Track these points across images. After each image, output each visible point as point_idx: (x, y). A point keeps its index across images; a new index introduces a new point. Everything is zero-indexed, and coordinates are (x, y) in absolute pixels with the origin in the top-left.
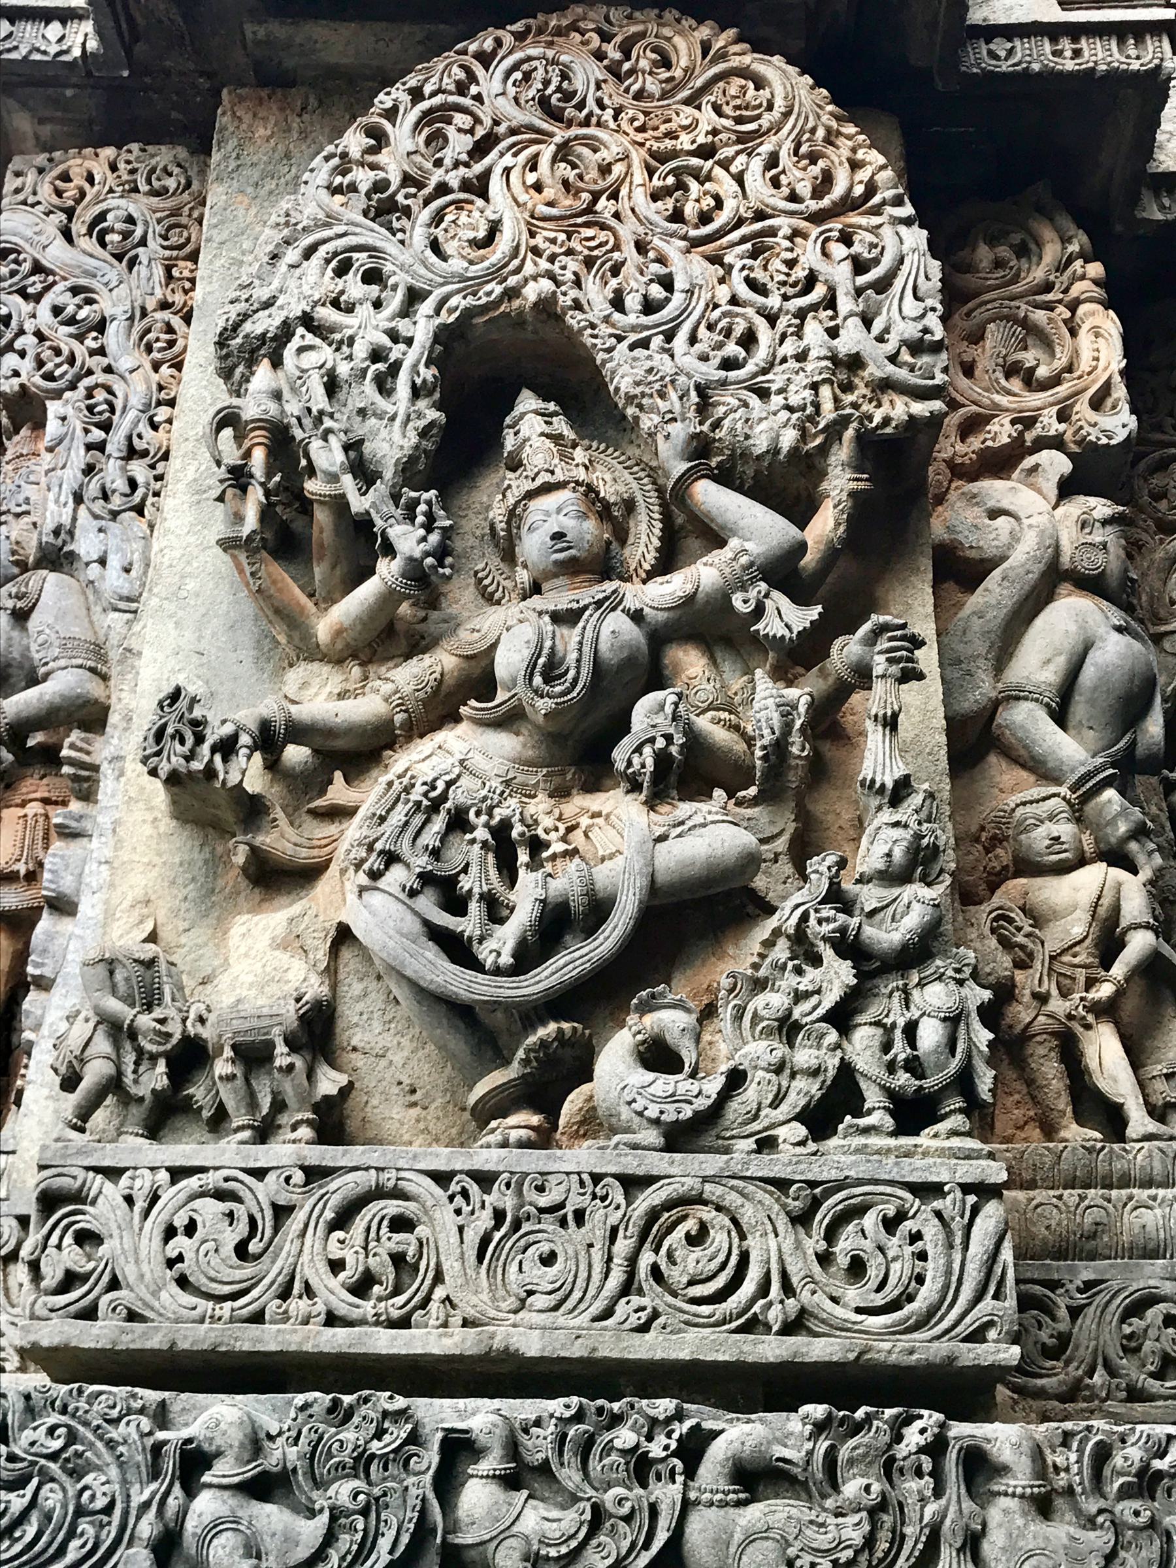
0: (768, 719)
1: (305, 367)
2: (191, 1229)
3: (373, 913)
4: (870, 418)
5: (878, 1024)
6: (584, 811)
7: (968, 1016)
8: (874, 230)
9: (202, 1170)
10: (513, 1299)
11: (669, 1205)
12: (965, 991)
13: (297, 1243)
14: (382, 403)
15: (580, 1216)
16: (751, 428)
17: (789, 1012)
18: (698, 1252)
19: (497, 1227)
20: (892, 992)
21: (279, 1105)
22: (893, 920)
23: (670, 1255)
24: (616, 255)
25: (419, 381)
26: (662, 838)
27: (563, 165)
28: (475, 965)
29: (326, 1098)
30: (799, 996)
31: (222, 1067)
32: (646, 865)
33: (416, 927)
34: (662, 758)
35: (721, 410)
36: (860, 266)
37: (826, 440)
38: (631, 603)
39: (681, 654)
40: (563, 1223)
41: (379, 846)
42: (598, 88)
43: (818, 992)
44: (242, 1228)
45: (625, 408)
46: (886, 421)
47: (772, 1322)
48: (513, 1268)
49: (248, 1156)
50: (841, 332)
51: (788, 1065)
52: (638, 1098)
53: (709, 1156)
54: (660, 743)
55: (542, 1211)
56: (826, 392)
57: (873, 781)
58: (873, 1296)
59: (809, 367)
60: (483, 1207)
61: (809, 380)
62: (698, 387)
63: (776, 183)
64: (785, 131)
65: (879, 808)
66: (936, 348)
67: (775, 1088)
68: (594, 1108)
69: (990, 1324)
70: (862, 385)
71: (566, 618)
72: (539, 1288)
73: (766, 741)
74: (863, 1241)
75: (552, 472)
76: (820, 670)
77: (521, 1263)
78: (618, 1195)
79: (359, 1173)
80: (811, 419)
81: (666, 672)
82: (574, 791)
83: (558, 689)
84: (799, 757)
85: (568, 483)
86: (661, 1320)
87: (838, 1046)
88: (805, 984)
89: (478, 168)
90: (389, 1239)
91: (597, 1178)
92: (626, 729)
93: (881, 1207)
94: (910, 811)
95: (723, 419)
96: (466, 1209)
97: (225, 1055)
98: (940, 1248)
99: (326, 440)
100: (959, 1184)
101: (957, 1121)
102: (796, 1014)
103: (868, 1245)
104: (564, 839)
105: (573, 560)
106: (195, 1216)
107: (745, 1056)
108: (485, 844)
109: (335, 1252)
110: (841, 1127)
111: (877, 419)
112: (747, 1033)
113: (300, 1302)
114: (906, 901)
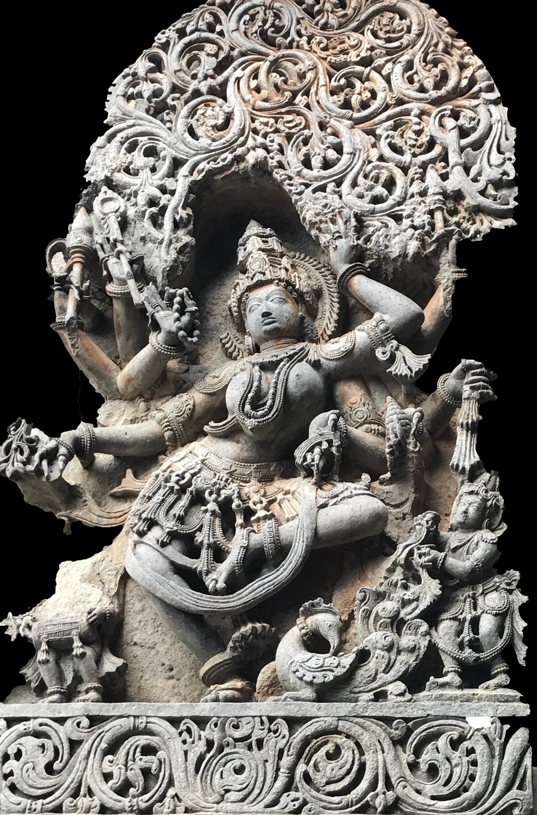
0: (393, 429)
1: (106, 211)
2: (18, 755)
3: (139, 558)
4: (467, 232)
5: (455, 619)
6: (280, 490)
7: (513, 612)
8: (474, 108)
9: (27, 719)
10: (216, 795)
11: (316, 735)
12: (511, 597)
13: (83, 763)
14: (154, 232)
15: (260, 743)
16: (389, 241)
17: (398, 613)
18: (333, 764)
19: (208, 750)
20: (465, 599)
21: (78, 679)
22: (467, 554)
23: (316, 766)
24: (306, 132)
25: (178, 218)
26: (324, 506)
27: (274, 74)
28: (203, 589)
29: (109, 674)
30: (405, 603)
31: (41, 656)
32: (312, 523)
33: (166, 565)
34: (326, 454)
35: (371, 229)
36: (463, 133)
37: (437, 247)
38: (312, 357)
39: (346, 388)
40: (250, 748)
41: (144, 516)
42: (298, 22)
43: (417, 599)
44: (50, 754)
45: (310, 231)
46: (478, 232)
47: (377, 806)
48: (217, 776)
49: (54, 710)
50: (450, 176)
51: (396, 646)
52: (300, 669)
53: (343, 704)
54: (325, 445)
55: (236, 740)
56: (438, 216)
57: (458, 466)
58: (442, 788)
59: (428, 200)
60: (200, 739)
61: (427, 209)
62: (356, 215)
63: (411, 81)
64: (418, 46)
65: (462, 483)
66: (509, 185)
67: (387, 661)
68: (277, 676)
69: (515, 805)
70: (463, 210)
71: (265, 367)
72: (233, 788)
73: (391, 443)
74: (437, 754)
75: (264, 274)
76: (433, 396)
77: (222, 772)
78: (284, 730)
79: (123, 719)
80: (428, 234)
81: (338, 400)
82: (276, 478)
83: (260, 413)
84: (413, 452)
85: (274, 280)
86: (308, 806)
87: (428, 633)
88: (408, 595)
89: (220, 79)
90: (141, 759)
91: (271, 719)
92: (305, 436)
93: (449, 733)
94: (480, 484)
95: (372, 235)
96: (189, 740)
97: (42, 649)
98: (485, 758)
99: (118, 258)
100: (499, 718)
101: (503, 679)
102: (402, 615)
103: (440, 757)
104: (267, 508)
105: (276, 329)
106: (21, 748)
107: (369, 641)
108: (213, 513)
109: (107, 768)
110: (428, 683)
111: (472, 232)
112: (371, 627)
113: (85, 799)
114: (476, 541)
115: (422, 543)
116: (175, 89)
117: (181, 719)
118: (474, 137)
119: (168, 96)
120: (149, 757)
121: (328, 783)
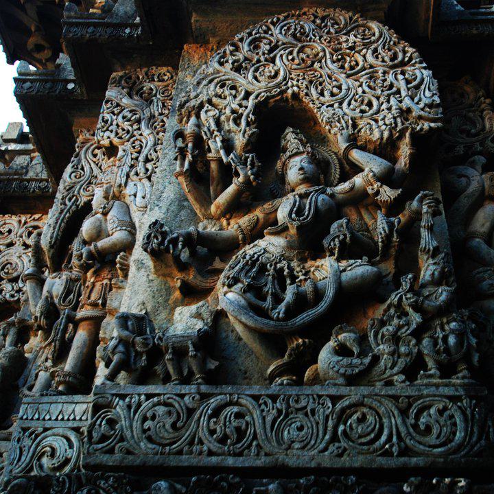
11: (349, 407)
24: (321, 79)
27: (301, 54)
36: (408, 82)
40: (306, 414)
42: (313, 30)
62: (352, 119)
63: (377, 57)
64: (380, 42)
65: (428, 259)
89: (272, 55)
101: (465, 372)
115: (408, 292)
116: (246, 59)
117: (261, 395)
118: (414, 83)
119: (243, 62)
120: (240, 420)
121: (360, 437)
